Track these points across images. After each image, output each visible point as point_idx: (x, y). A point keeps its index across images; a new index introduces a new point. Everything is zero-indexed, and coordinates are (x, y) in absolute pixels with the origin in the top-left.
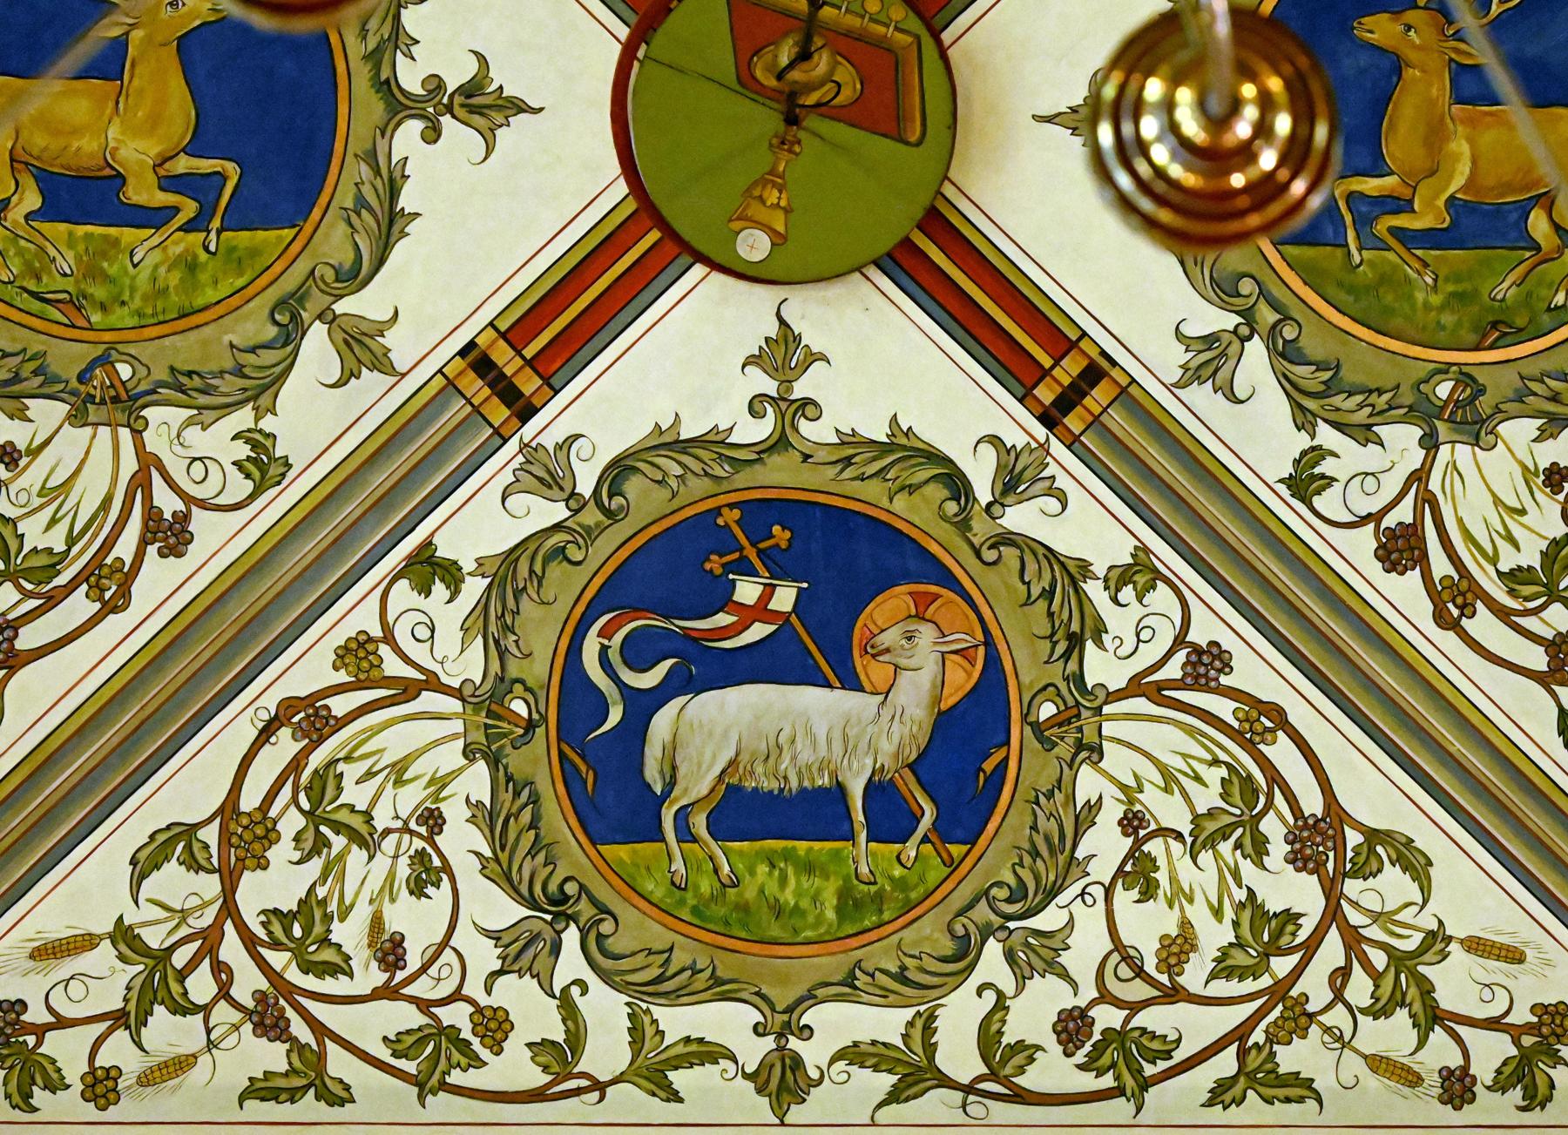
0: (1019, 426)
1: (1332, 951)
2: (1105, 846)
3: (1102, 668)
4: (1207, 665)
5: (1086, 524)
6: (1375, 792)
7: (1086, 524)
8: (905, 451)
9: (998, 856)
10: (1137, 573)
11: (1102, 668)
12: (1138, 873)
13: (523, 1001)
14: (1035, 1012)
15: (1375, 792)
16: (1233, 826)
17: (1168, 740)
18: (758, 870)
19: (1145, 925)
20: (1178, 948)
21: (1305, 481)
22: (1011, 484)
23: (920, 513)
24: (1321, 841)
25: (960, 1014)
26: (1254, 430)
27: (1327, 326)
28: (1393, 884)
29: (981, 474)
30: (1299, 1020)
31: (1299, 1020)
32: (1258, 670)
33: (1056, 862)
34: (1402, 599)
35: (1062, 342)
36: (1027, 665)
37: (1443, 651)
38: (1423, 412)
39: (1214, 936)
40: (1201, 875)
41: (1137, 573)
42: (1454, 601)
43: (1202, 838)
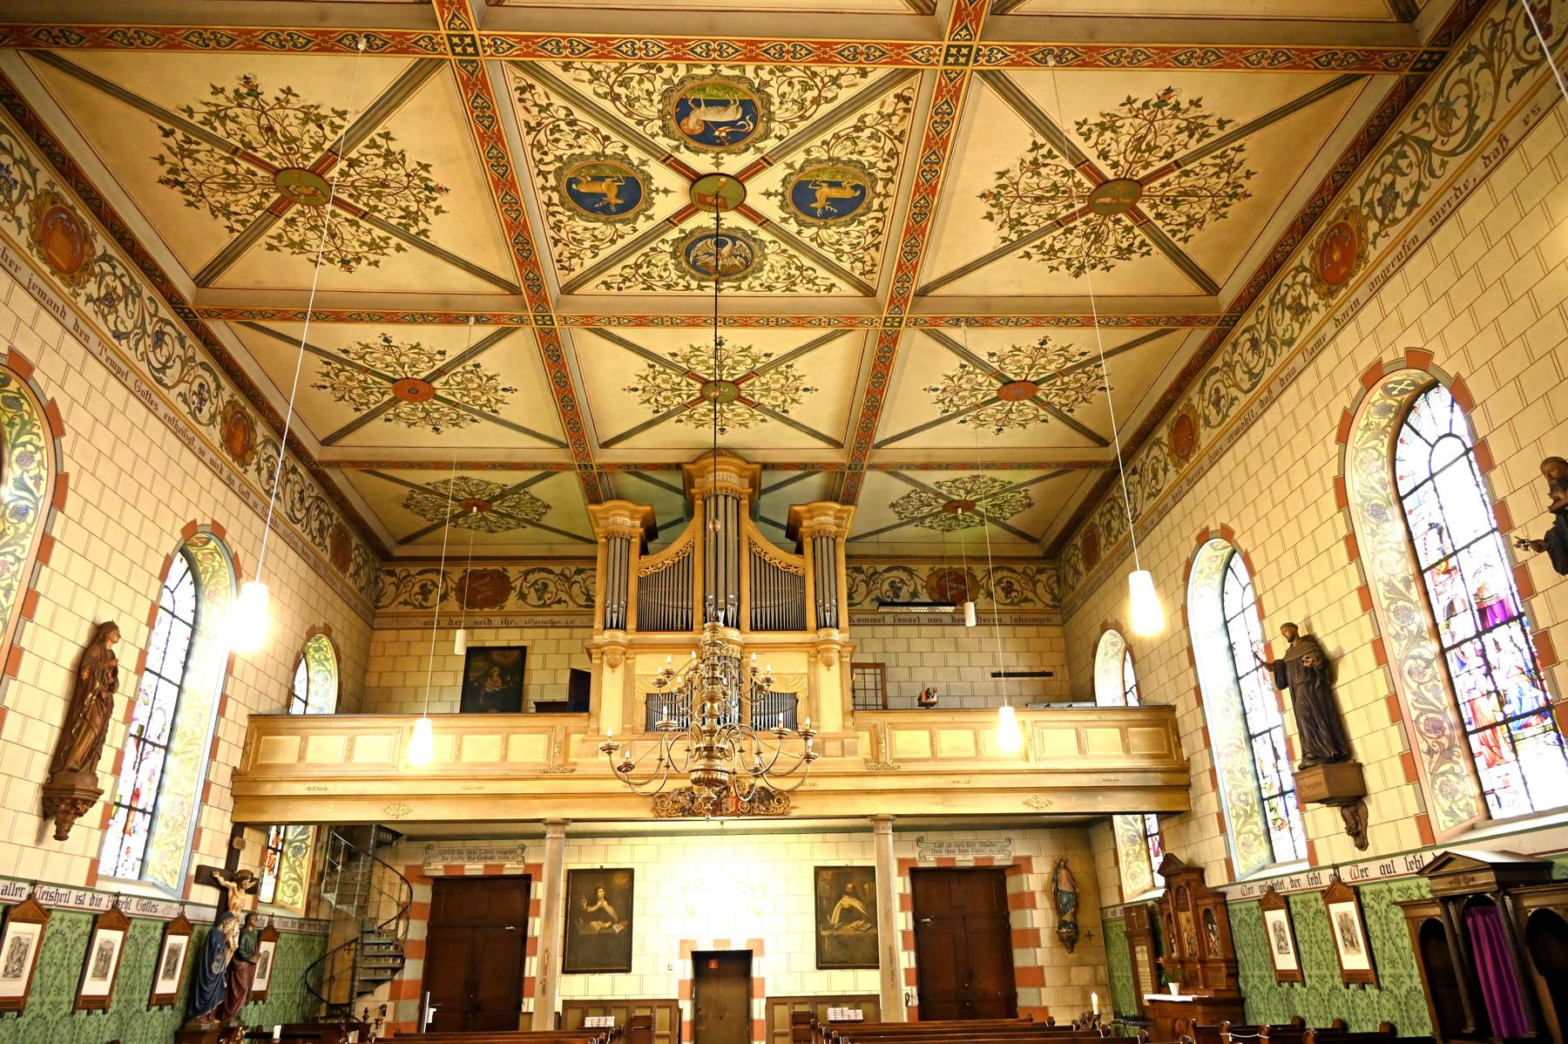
0: (676, 155)
1: (611, 81)
2: (656, 97)
3: (660, 123)
4: (640, 123)
5: (664, 142)
6: (607, 105)
7: (664, 142)
8: (697, 152)
9: (676, 97)
10: (653, 136)
11: (660, 123)
12: (649, 93)
13: (766, 77)
14: (667, 73)
15: (607, 105)
16: (631, 102)
17: (645, 112)
18: (722, 95)
19: (647, 85)
20: (641, 82)
21: (625, 147)
22: (677, 148)
23: (693, 144)
24: (616, 98)
25: (682, 71)
26: (634, 154)
27: (625, 166)
28: (601, 91)
29: (682, 148)
30: (616, 70)
31: (616, 70)
32: (631, 123)
33: (665, 96)
34: (605, 131)
35: (670, 165)
36: (672, 124)
37: (597, 124)
38: (606, 156)
39: (634, 83)
40: (637, 93)
41: (653, 136)
42: (595, 131)
43: (638, 99)
